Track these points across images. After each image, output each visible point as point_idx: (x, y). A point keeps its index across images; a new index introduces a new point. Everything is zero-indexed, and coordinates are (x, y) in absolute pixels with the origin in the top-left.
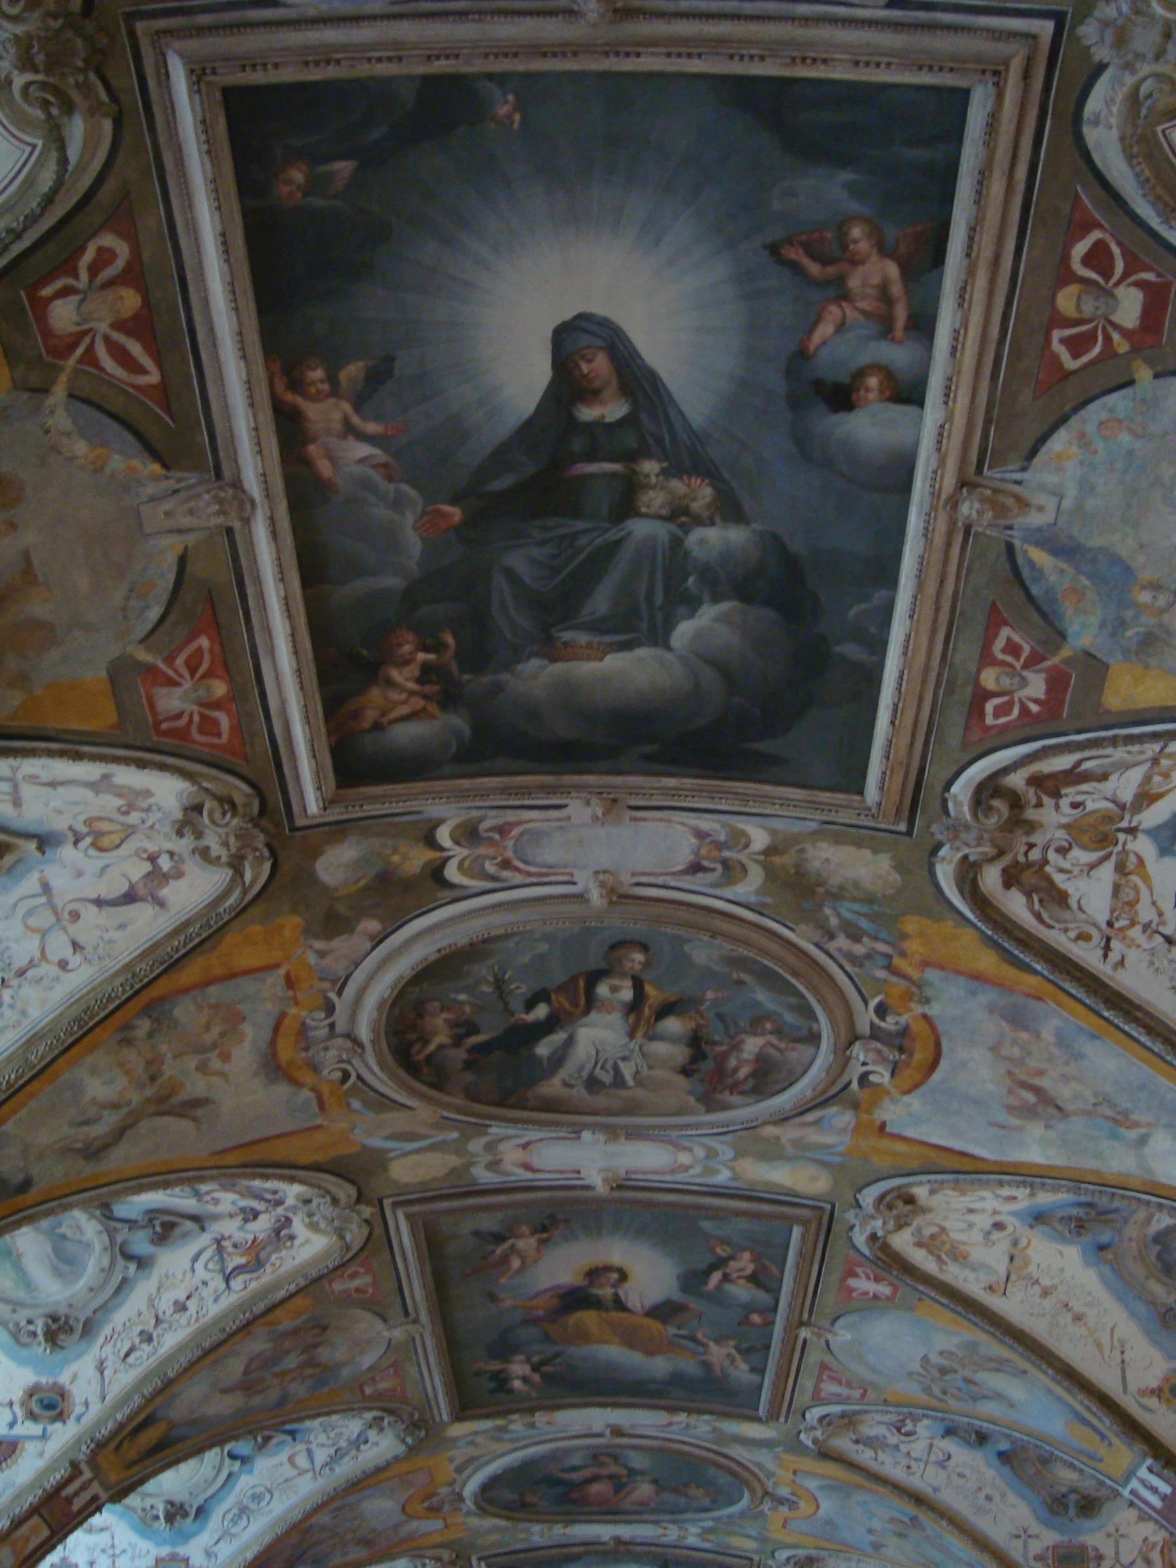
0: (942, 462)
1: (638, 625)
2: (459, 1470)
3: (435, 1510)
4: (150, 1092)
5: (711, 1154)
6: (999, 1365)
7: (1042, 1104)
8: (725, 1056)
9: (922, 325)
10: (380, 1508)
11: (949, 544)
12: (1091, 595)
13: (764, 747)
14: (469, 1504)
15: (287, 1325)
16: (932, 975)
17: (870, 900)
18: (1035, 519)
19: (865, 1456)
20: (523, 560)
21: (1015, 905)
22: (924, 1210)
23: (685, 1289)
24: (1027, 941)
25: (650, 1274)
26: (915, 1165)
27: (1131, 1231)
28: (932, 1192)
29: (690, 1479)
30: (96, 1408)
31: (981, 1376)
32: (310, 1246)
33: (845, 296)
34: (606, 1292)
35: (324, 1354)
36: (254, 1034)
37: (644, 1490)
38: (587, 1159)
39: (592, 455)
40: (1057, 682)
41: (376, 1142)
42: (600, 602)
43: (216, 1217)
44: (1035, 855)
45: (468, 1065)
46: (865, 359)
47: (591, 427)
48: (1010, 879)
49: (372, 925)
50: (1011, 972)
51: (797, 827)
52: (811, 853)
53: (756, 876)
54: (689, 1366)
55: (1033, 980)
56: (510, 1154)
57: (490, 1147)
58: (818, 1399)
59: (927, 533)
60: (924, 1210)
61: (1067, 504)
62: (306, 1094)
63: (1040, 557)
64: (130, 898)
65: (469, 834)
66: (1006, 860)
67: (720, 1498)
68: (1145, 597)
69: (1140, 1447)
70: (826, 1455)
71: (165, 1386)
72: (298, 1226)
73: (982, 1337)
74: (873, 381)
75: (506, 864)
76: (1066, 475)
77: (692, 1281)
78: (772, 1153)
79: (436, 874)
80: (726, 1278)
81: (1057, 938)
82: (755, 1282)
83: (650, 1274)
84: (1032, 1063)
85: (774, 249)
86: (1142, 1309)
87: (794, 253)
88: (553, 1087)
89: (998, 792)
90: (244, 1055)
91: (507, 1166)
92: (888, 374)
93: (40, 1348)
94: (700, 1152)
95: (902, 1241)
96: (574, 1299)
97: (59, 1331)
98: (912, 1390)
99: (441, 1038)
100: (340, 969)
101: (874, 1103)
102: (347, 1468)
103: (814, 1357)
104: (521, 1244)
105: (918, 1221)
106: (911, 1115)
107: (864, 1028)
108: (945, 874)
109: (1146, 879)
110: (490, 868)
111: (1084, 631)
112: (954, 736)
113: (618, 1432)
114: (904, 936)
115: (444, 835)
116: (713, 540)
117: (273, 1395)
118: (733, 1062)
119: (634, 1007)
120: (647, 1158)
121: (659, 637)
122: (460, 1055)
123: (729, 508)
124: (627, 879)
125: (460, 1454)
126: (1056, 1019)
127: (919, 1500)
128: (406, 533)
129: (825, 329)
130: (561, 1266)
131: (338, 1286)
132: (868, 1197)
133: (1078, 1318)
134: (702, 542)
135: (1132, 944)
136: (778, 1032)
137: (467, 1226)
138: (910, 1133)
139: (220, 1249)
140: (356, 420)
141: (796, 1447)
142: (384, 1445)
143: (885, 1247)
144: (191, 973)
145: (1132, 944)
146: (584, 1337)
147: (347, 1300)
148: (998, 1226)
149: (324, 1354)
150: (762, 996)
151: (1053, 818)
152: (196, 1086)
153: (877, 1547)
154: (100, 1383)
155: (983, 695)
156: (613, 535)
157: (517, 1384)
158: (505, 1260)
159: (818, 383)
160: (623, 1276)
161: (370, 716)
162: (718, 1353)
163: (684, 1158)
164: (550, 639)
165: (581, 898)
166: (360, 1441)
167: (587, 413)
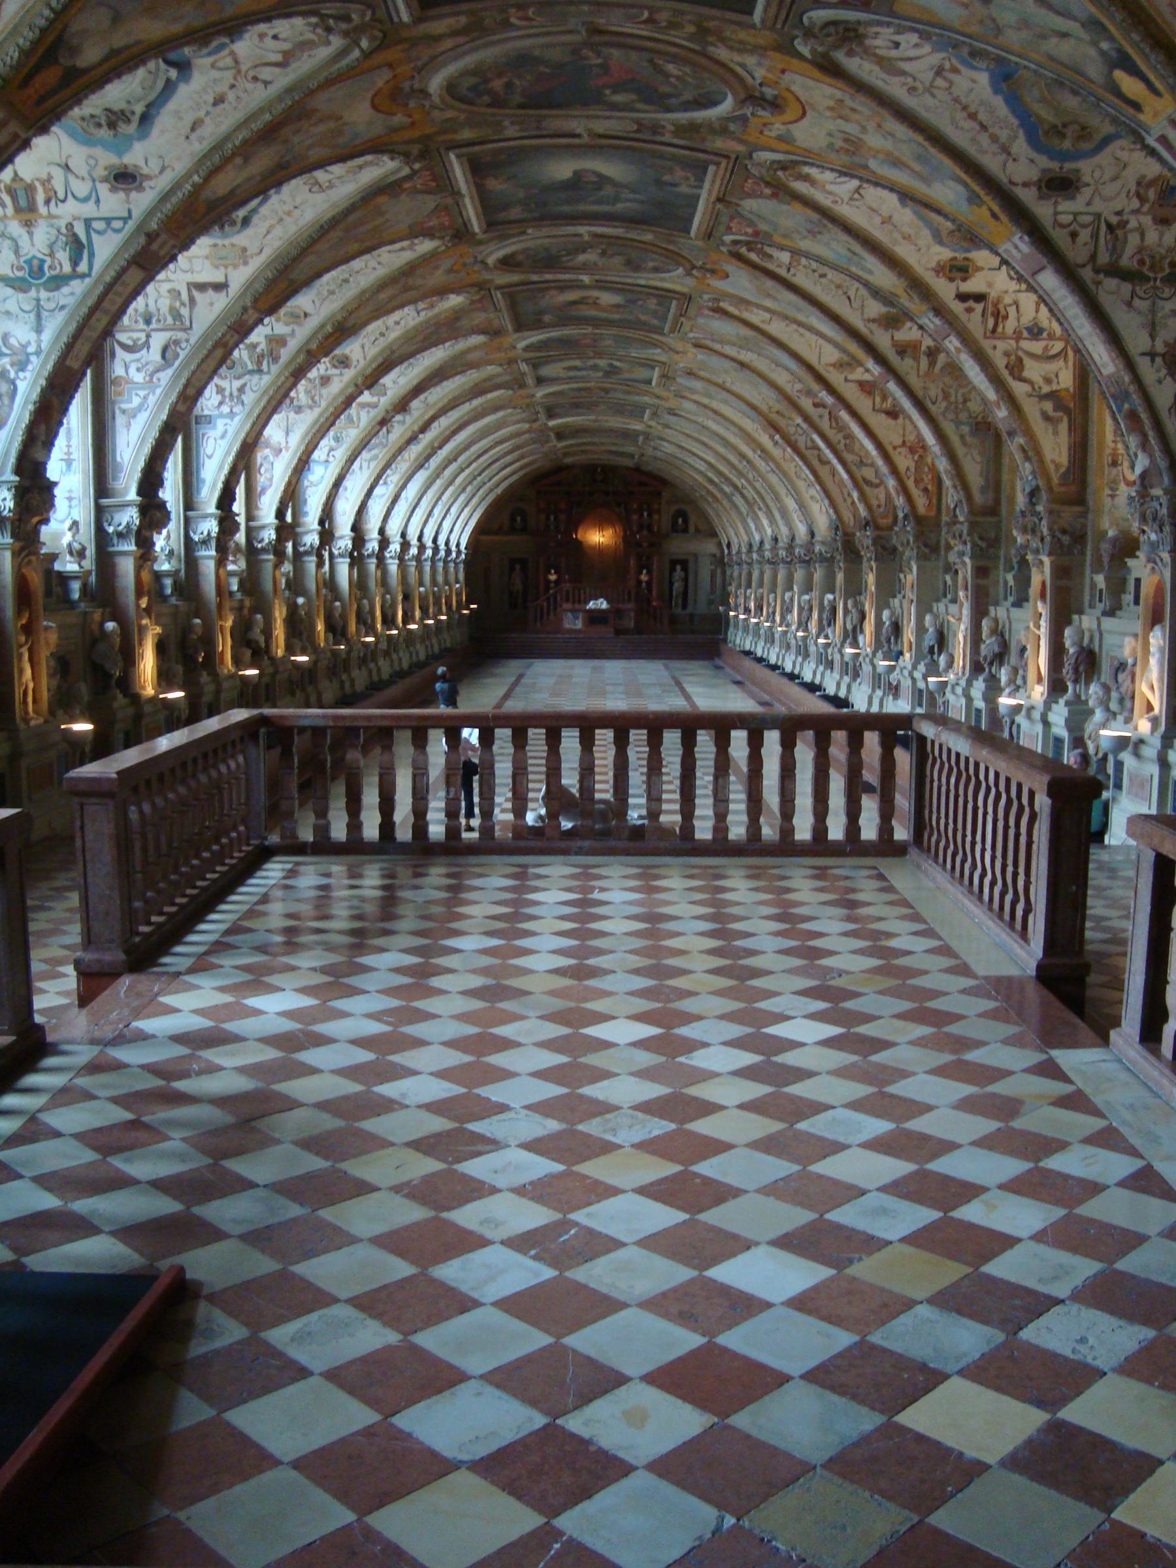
7: (769, 296)
19: (718, 347)
21: (753, 256)
25: (607, 298)
30: (362, 363)
40: (756, 234)
48: (749, 250)
54: (631, 317)
64: (403, 249)
70: (697, 346)
71: (390, 349)
81: (770, 266)
119: (604, 253)
126: (769, 283)
127: (743, 365)
132: (706, 297)
141: (682, 339)
162: (643, 318)
165: (580, 235)
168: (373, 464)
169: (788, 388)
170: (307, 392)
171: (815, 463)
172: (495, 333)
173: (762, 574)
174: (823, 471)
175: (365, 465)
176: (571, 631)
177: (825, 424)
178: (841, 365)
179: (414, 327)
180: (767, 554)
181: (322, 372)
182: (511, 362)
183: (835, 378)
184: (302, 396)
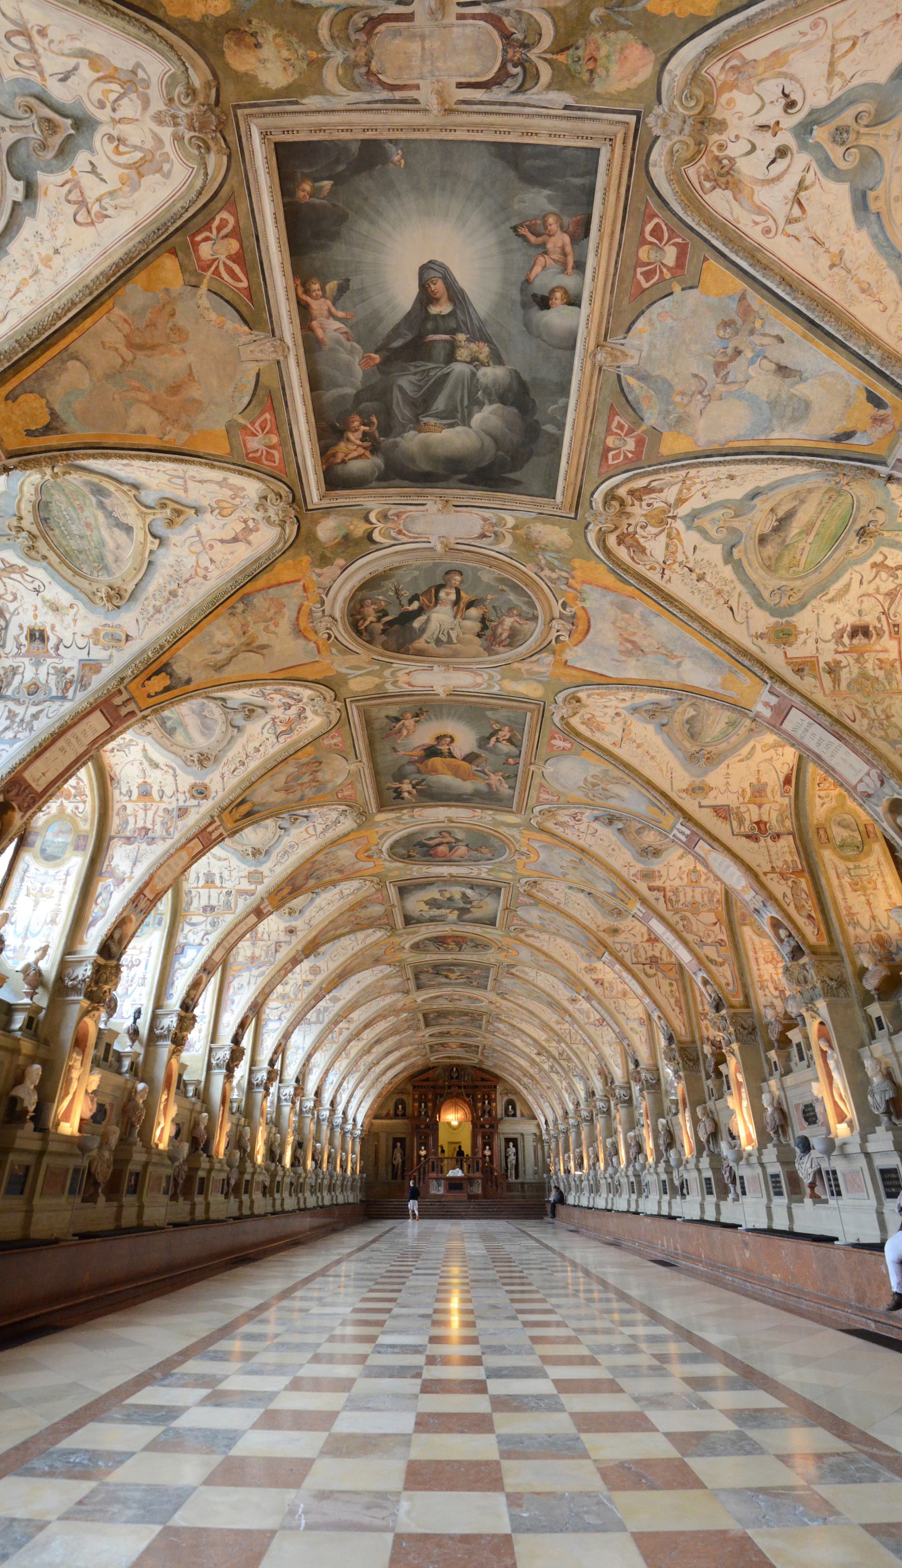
0: (589, 333)
1: (456, 415)
2: (380, 838)
3: (370, 857)
4: (243, 640)
5: (491, 677)
6: (617, 781)
7: (634, 649)
8: (496, 627)
9: (580, 266)
10: (345, 855)
11: (592, 376)
12: (654, 399)
13: (512, 476)
14: (385, 855)
15: (304, 760)
16: (586, 587)
17: (558, 551)
18: (630, 363)
19: (559, 831)
20: (406, 382)
21: (622, 553)
22: (585, 706)
23: (480, 747)
24: (627, 570)
26: (580, 682)
27: (677, 717)
28: (589, 696)
29: (483, 845)
30: (221, 794)
31: (610, 787)
32: (314, 722)
33: (546, 253)
34: (444, 748)
35: (320, 776)
36: (289, 613)
37: (462, 850)
38: (436, 680)
39: (436, 331)
40: (640, 442)
41: (343, 670)
42: (440, 404)
43: (273, 707)
44: (631, 529)
45: (384, 631)
46: (554, 284)
47: (435, 316)
49: (341, 562)
50: (621, 585)
51: (527, 516)
52: (533, 528)
53: (509, 539)
54: (482, 786)
55: (631, 589)
56: (402, 677)
57: (393, 674)
58: (539, 803)
59: (582, 369)
60: (585, 706)
61: (644, 354)
62: (312, 645)
63: (632, 381)
65: (384, 517)
66: (618, 532)
67: (496, 852)
68: (678, 399)
69: (677, 813)
70: (543, 830)
72: (309, 713)
73: (611, 767)
74: (558, 295)
75: (400, 532)
76: (645, 340)
77: (483, 742)
78: (517, 677)
79: (369, 537)
80: (498, 740)
81: (641, 569)
82: (509, 739)
83: (465, 740)
84: (631, 629)
85: (515, 229)
86: (680, 754)
87: (524, 231)
88: (420, 644)
89: (614, 498)
90: (285, 625)
91: (400, 684)
92: (566, 292)
93: (196, 768)
94: (486, 677)
95: (575, 721)
96: (431, 752)
97: (203, 760)
98: (579, 795)
99: (372, 618)
100: (327, 583)
101: (562, 651)
102: (331, 835)
103: (537, 780)
104: (407, 723)
105: (582, 711)
106: (579, 656)
107: (556, 614)
108: (592, 537)
109: (680, 541)
110: (393, 534)
111: (652, 417)
112: (595, 469)
113: (451, 820)
114: (574, 569)
115: (372, 517)
116: (490, 374)
117: (298, 795)
118: (499, 631)
119: (456, 603)
120: (462, 680)
121: (466, 421)
122: (380, 626)
123: (497, 359)
124: (453, 541)
125: (381, 830)
127: (582, 850)
128: (355, 367)
129: (537, 269)
130: (423, 734)
131: (326, 742)
133: (652, 758)
134: (485, 375)
135: (675, 572)
136: (519, 615)
137: (383, 713)
138: (578, 665)
139: (274, 723)
140: (333, 310)
141: (530, 827)
142: (348, 824)
143: (567, 724)
144: (261, 582)
145: (675, 572)
146: (435, 771)
147: (330, 749)
148: (618, 714)
149: (320, 776)
150: (512, 597)
151: (638, 511)
152: (263, 639)
153: (565, 875)
154: (222, 783)
155: (608, 450)
156: (445, 371)
157: (406, 795)
158: (400, 731)
159: (534, 296)
160: (452, 740)
161: (340, 456)
163: (479, 680)
164: (418, 421)
165: (432, 549)
166: (337, 822)
167: (434, 310)
168: (260, 979)
169: (624, 872)
170: (163, 824)
171: (642, 976)
172: (363, 814)
173: (578, 1134)
174: (650, 983)
175: (253, 980)
176: (435, 1196)
177: (661, 907)
178: (693, 790)
179: (274, 755)
180: (584, 1114)
181: (181, 803)
182: (381, 880)
183: (689, 804)
184: (158, 828)
